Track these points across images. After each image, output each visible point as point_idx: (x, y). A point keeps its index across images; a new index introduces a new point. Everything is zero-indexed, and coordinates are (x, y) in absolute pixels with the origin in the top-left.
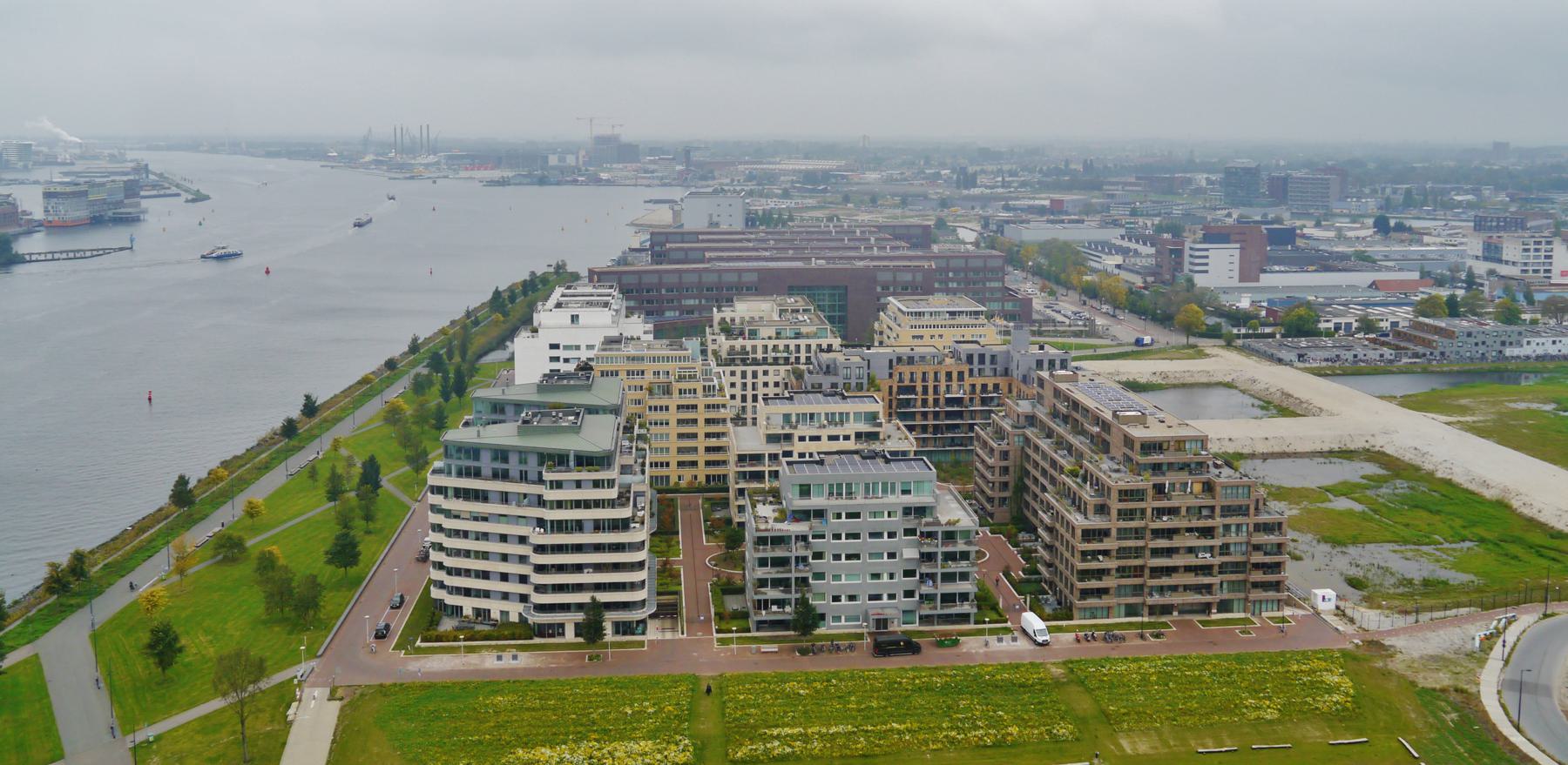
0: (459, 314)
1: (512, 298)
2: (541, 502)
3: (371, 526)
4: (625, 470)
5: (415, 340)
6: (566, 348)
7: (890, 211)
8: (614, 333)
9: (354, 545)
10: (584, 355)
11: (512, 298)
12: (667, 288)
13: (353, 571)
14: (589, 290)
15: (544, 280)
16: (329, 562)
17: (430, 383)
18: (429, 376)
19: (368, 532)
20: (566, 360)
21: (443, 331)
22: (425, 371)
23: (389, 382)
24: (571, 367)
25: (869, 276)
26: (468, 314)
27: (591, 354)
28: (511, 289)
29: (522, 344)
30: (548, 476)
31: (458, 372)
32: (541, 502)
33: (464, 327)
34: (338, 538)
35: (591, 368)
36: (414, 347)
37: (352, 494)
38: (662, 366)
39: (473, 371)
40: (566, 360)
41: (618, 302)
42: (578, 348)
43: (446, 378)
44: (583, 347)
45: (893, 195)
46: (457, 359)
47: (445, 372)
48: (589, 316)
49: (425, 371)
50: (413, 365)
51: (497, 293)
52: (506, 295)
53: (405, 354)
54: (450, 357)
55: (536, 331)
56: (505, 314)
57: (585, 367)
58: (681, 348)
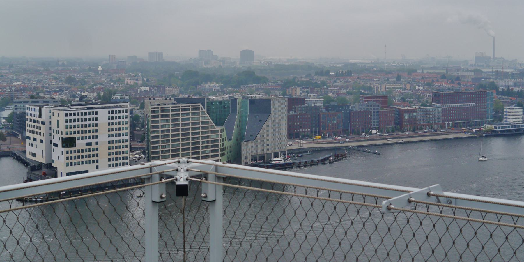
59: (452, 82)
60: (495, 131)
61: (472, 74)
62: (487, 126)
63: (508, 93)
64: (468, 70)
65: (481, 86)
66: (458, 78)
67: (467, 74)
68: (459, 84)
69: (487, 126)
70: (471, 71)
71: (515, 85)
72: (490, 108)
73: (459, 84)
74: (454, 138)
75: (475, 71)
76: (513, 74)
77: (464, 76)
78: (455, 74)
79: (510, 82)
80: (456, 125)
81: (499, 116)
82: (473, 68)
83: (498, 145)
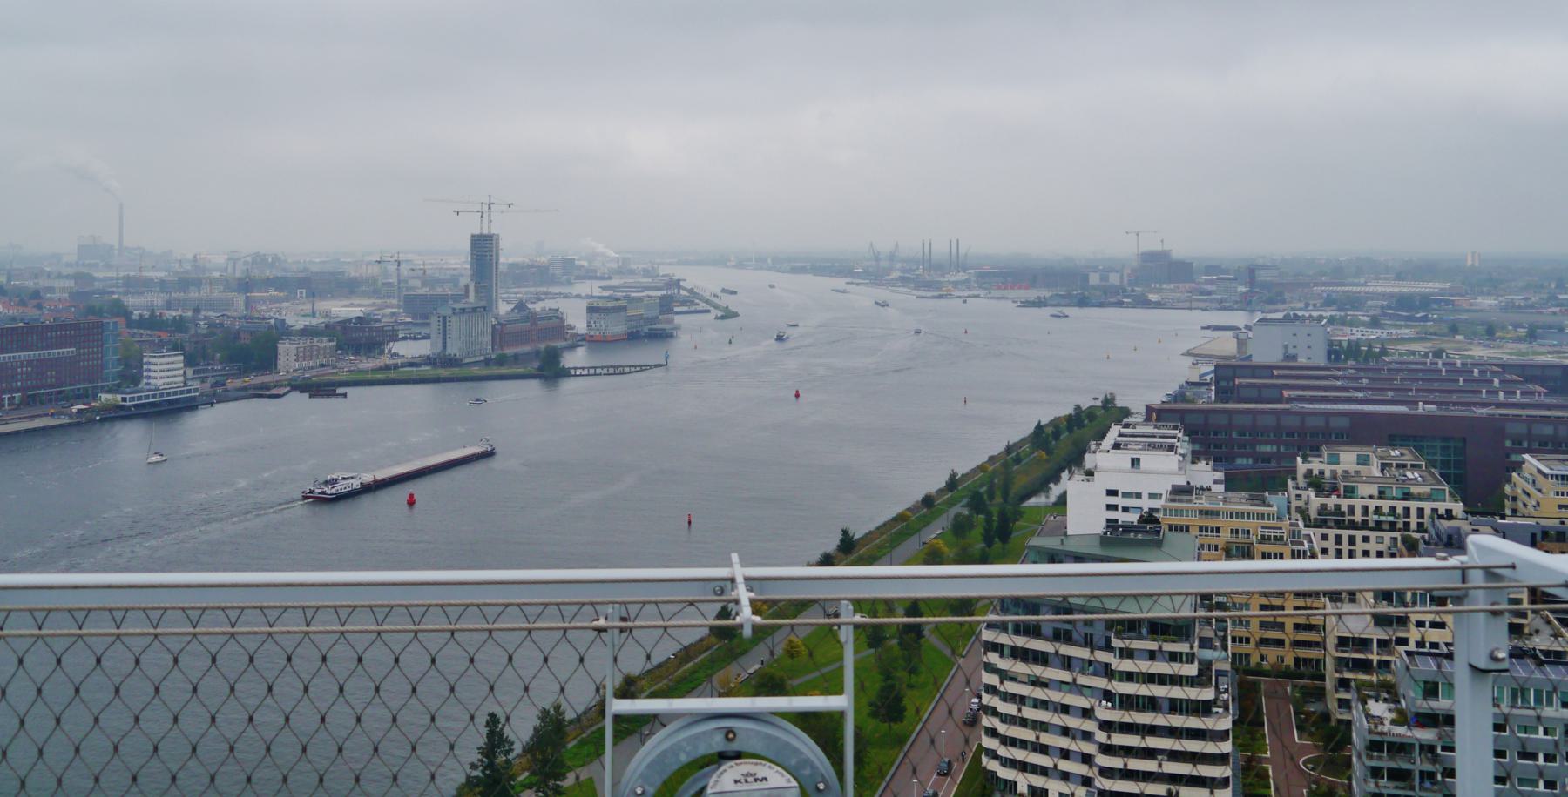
0: (998, 448)
1: (1056, 435)
2: (1108, 671)
3: (914, 679)
4: (1205, 643)
5: (953, 476)
6: (1125, 495)
7: (1511, 345)
8: (1181, 481)
9: (899, 699)
10: (1146, 504)
11: (1056, 435)
12: (1243, 430)
13: (896, 727)
14: (1150, 429)
15: (1091, 413)
16: (874, 715)
17: (972, 526)
18: (969, 518)
19: (911, 687)
20: (1125, 510)
21: (981, 468)
22: (966, 512)
23: (925, 522)
24: (1133, 518)
25: (1494, 429)
26: (1009, 449)
27: (1156, 504)
28: (1055, 423)
29: (1071, 484)
30: (1116, 643)
31: (1002, 515)
32: (1108, 671)
33: (1005, 465)
34: (883, 690)
35: (1157, 521)
36: (953, 483)
37: (895, 642)
38: (1240, 524)
39: (1019, 514)
40: (1125, 510)
41: (1184, 447)
42: (1139, 496)
43: (989, 521)
44: (1145, 496)
45: (1516, 326)
46: (998, 500)
47: (989, 515)
48: (1150, 460)
49: (966, 512)
50: (951, 503)
51: (1039, 428)
52: (1049, 430)
53: (941, 491)
54: (991, 497)
55: (1090, 473)
56: (1049, 453)
57: (1150, 518)
58: (1264, 503)
59: (23, 303)
60: (122, 408)
61: (71, 283)
62: (105, 397)
63: (152, 322)
64: (60, 276)
65: (91, 310)
66: (36, 294)
67: (57, 284)
68: (39, 307)
69: (105, 397)
70: (67, 277)
71: (169, 305)
72: (111, 358)
73: (39, 307)
74: (27, 431)
75: (78, 277)
76: (162, 282)
77: (51, 290)
78: (31, 284)
79: (157, 300)
80: (30, 401)
81: (131, 374)
82: (71, 271)
83: (130, 440)
